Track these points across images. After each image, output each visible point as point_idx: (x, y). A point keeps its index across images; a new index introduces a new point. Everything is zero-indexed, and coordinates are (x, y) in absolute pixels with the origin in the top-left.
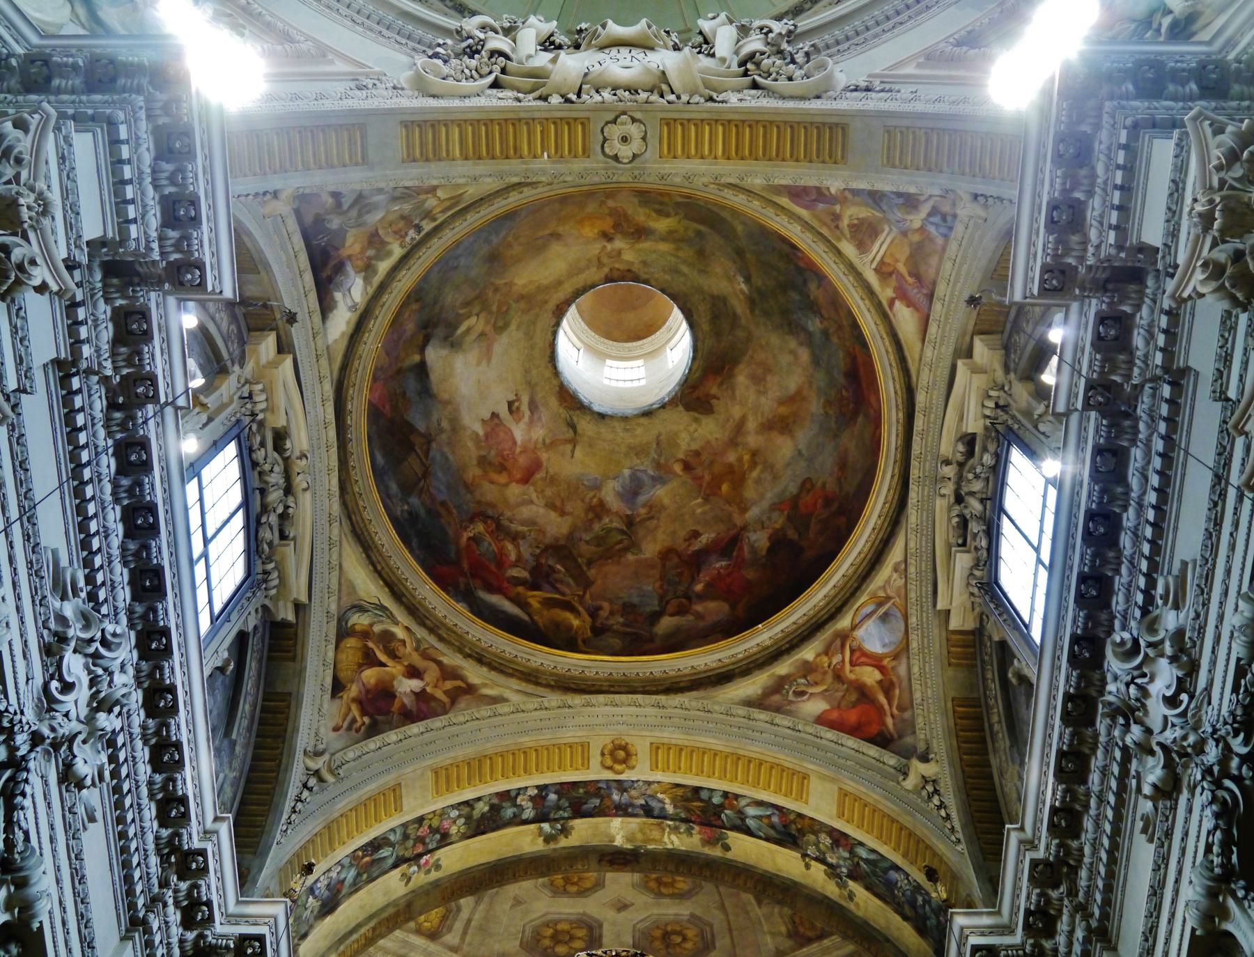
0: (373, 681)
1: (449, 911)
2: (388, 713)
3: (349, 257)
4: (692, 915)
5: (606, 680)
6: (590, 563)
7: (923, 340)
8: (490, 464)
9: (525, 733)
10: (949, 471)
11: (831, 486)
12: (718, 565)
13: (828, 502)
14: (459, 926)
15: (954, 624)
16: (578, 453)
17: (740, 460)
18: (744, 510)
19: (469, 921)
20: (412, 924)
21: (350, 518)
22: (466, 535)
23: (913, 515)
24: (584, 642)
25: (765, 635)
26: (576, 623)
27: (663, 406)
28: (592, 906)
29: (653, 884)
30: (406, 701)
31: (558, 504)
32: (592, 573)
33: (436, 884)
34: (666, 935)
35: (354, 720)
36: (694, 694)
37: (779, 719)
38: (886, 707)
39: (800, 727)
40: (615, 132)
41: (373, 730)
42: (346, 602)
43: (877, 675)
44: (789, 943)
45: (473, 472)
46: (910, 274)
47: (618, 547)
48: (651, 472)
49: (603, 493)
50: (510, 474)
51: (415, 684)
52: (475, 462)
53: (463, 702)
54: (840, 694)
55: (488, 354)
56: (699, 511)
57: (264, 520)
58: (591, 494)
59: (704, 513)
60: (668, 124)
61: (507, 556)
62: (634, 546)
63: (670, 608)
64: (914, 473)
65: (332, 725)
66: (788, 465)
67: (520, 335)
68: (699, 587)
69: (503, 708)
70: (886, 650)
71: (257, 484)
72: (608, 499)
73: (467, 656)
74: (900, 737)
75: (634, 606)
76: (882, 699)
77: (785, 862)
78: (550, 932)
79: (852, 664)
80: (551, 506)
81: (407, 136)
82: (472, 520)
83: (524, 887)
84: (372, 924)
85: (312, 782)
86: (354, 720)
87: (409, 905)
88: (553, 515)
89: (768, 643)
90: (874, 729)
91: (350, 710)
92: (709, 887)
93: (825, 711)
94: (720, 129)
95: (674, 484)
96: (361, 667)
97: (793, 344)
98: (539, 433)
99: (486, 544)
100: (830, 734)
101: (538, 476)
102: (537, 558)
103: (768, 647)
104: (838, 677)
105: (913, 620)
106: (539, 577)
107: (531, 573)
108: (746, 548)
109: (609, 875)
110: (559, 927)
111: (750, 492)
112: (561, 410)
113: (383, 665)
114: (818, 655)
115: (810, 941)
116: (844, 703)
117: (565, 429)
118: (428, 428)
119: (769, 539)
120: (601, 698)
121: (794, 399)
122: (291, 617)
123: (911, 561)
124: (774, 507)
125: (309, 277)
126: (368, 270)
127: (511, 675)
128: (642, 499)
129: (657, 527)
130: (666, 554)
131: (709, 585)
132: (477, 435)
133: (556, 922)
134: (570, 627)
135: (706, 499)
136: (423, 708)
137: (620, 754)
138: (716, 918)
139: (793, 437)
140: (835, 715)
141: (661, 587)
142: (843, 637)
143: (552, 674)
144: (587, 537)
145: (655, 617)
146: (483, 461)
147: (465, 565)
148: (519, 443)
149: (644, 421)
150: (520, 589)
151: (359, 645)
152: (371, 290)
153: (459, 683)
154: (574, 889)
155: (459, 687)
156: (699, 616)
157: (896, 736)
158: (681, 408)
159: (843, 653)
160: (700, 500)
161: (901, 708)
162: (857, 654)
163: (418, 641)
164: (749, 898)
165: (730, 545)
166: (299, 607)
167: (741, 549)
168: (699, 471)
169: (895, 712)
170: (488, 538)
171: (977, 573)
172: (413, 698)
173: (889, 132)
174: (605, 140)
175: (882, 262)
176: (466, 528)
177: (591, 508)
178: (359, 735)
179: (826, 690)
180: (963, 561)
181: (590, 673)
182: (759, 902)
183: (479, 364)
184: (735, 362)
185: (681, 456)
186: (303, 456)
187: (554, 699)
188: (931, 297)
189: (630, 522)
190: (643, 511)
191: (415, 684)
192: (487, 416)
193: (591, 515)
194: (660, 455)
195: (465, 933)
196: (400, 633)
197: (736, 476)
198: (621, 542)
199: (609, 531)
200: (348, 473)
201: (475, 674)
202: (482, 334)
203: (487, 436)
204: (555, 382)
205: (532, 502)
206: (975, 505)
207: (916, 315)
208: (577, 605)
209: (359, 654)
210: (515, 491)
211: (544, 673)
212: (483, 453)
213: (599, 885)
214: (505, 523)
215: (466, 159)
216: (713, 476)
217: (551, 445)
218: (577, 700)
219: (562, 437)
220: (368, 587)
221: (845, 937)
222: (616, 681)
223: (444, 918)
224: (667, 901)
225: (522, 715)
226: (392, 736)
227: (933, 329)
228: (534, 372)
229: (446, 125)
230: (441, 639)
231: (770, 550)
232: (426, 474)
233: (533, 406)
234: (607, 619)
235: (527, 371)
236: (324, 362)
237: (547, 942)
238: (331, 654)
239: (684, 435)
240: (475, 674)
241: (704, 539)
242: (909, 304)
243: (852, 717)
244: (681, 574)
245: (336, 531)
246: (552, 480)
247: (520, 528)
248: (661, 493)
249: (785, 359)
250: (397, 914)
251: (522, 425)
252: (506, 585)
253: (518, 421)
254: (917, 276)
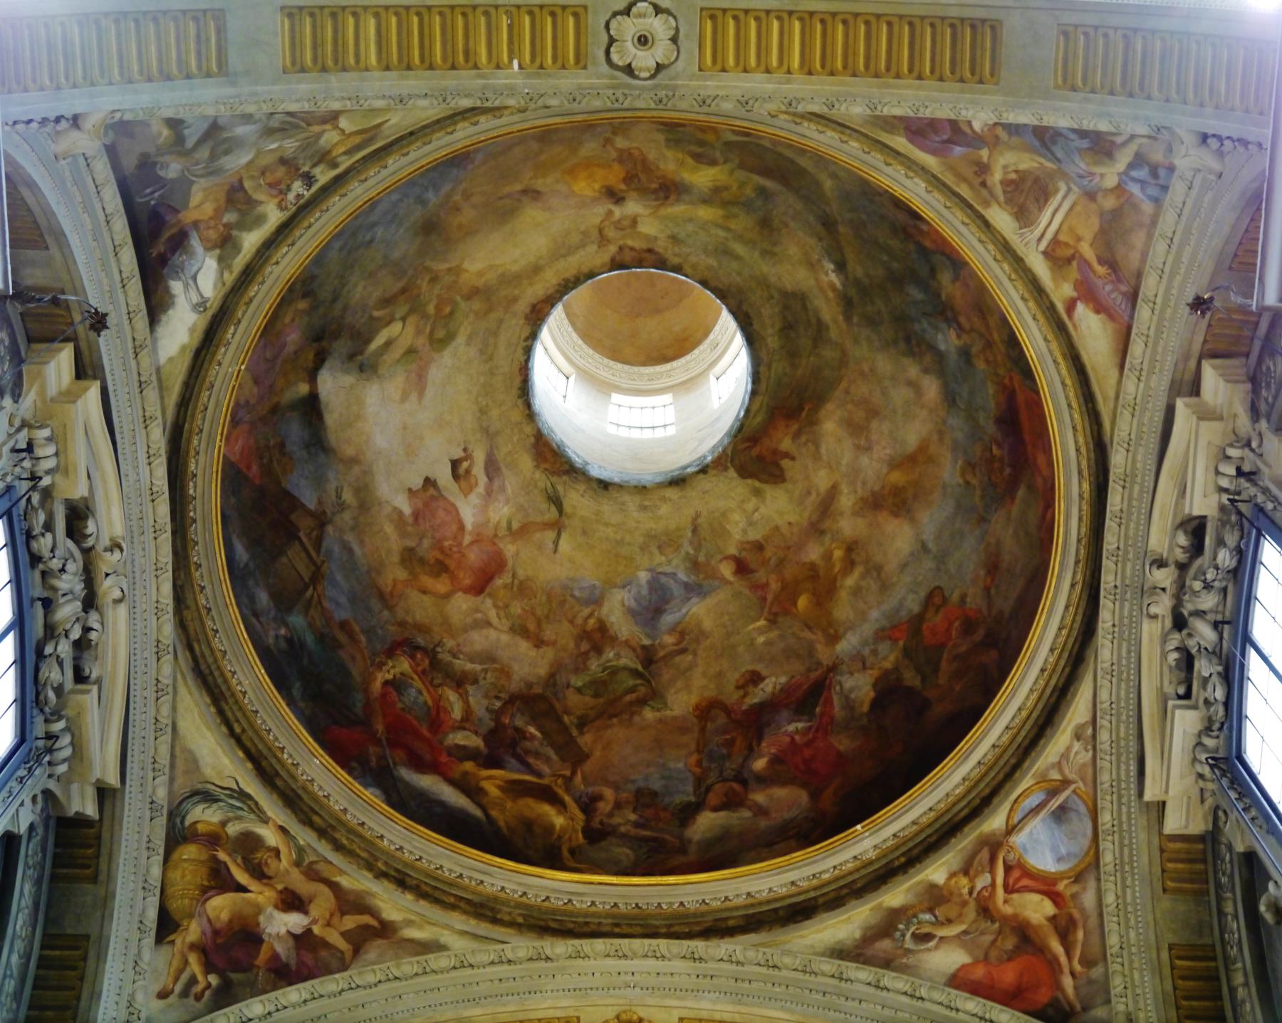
0: (225, 916)
2: (247, 967)
3: (196, 224)
5: (608, 915)
6: (582, 724)
7: (1122, 367)
8: (422, 561)
9: (475, 1001)
10: (1163, 577)
11: (975, 601)
12: (791, 728)
13: (969, 626)
15: (1174, 823)
16: (564, 545)
17: (828, 556)
18: (834, 639)
21: (190, 648)
22: (381, 677)
23: (1105, 649)
24: (572, 852)
25: (866, 842)
26: (559, 821)
27: (704, 470)
30: (280, 948)
31: (532, 627)
32: (585, 740)
35: (193, 981)
36: (752, 938)
37: (888, 978)
38: (1063, 959)
39: (923, 993)
41: (224, 997)
42: (183, 785)
43: (1049, 908)
45: (394, 574)
46: (1101, 261)
47: (628, 698)
48: (682, 576)
49: (605, 610)
50: (453, 578)
51: (295, 921)
52: (396, 558)
53: (374, 950)
54: (988, 938)
55: (419, 382)
56: (761, 639)
57: (49, 649)
58: (587, 611)
59: (769, 643)
60: (713, 17)
61: (448, 712)
62: (654, 696)
63: (713, 799)
64: (1108, 579)
65: (157, 987)
66: (903, 566)
67: (473, 352)
68: (760, 764)
69: (437, 961)
70: (1063, 867)
71: (38, 592)
72: (613, 619)
73: (381, 875)
74: (1085, 1009)
75: (654, 794)
76: (1056, 946)
79: (1008, 889)
80: (520, 630)
81: (292, 30)
82: (390, 652)
86: (193, 981)
88: (524, 646)
89: (872, 855)
90: (1043, 996)
91: (186, 963)
93: (963, 967)
94: (797, 25)
95: (722, 595)
96: (206, 892)
97: (913, 371)
98: (501, 512)
99: (413, 692)
100: (973, 1004)
101: (499, 582)
102: (497, 715)
103: (871, 863)
104: (985, 911)
105: (1105, 818)
106: (500, 746)
107: (486, 739)
108: (835, 698)
111: (842, 609)
112: (538, 475)
113: (243, 889)
114: (952, 875)
116: (994, 954)
117: (544, 506)
118: (320, 503)
119: (875, 685)
120: (600, 944)
121: (913, 460)
122: (91, 810)
123: (1103, 722)
124: (882, 635)
125: (128, 256)
126: (225, 244)
127: (453, 907)
128: (668, 619)
129: (690, 668)
130: (706, 710)
131: (775, 761)
132: (400, 513)
134: (550, 829)
135: (773, 621)
136: (307, 962)
139: (912, 520)
140: (979, 973)
141: (699, 763)
142: (994, 845)
143: (519, 905)
144: (578, 681)
145: (688, 812)
146: (409, 557)
147: (380, 728)
148: (469, 527)
149: (671, 493)
150: (469, 766)
151: (204, 856)
152: (230, 278)
153: (366, 919)
155: (366, 927)
156: (761, 811)
157: (1078, 1007)
158: (732, 473)
159: (992, 872)
160: (762, 623)
161: (1087, 962)
162: (1016, 874)
163: (301, 851)
165: (810, 695)
166: (104, 793)
167: (829, 702)
168: (761, 576)
169: (1078, 968)
170: (418, 683)
171: (1209, 742)
172: (291, 942)
173: (1065, 34)
174: (612, 41)
175: (1055, 241)
176: (380, 666)
177: (584, 635)
178: (200, 1006)
179: (965, 932)
180: (1186, 722)
181: (581, 905)
183: (404, 398)
184: (820, 400)
185: (732, 550)
186: (115, 546)
187: (522, 946)
188: (1133, 297)
189: (649, 657)
190: (669, 640)
191: (295, 921)
192: (417, 483)
193: (585, 646)
194: (698, 548)
196: (270, 837)
197: (821, 584)
198: (632, 690)
199: (614, 672)
200: (188, 574)
201: (393, 904)
202: (411, 351)
203: (416, 515)
204: (528, 430)
205: (489, 624)
206: (1205, 633)
207: (1110, 326)
208: (561, 792)
209: (204, 871)
210: (461, 605)
211: (506, 903)
212: (410, 543)
214: (445, 657)
215: (387, 68)
216: (785, 583)
217: (521, 532)
218: (559, 947)
219: (539, 519)
220: (219, 761)
222: (624, 916)
225: (469, 971)
226: (255, 1007)
227: (1137, 348)
228: (495, 413)
229: (355, 14)
230: (338, 847)
231: (875, 704)
232: (317, 576)
233: (492, 467)
234: (610, 815)
235: (483, 411)
236: (152, 394)
238: (156, 871)
239: (736, 517)
240: (393, 904)
241: (769, 686)
242: (1099, 308)
243: (1008, 975)
244: (730, 743)
245: (167, 669)
246: (523, 589)
247: (469, 666)
248: (701, 611)
249: (900, 395)
251: (474, 498)
252: (444, 759)
253: (466, 493)
254: (1112, 264)
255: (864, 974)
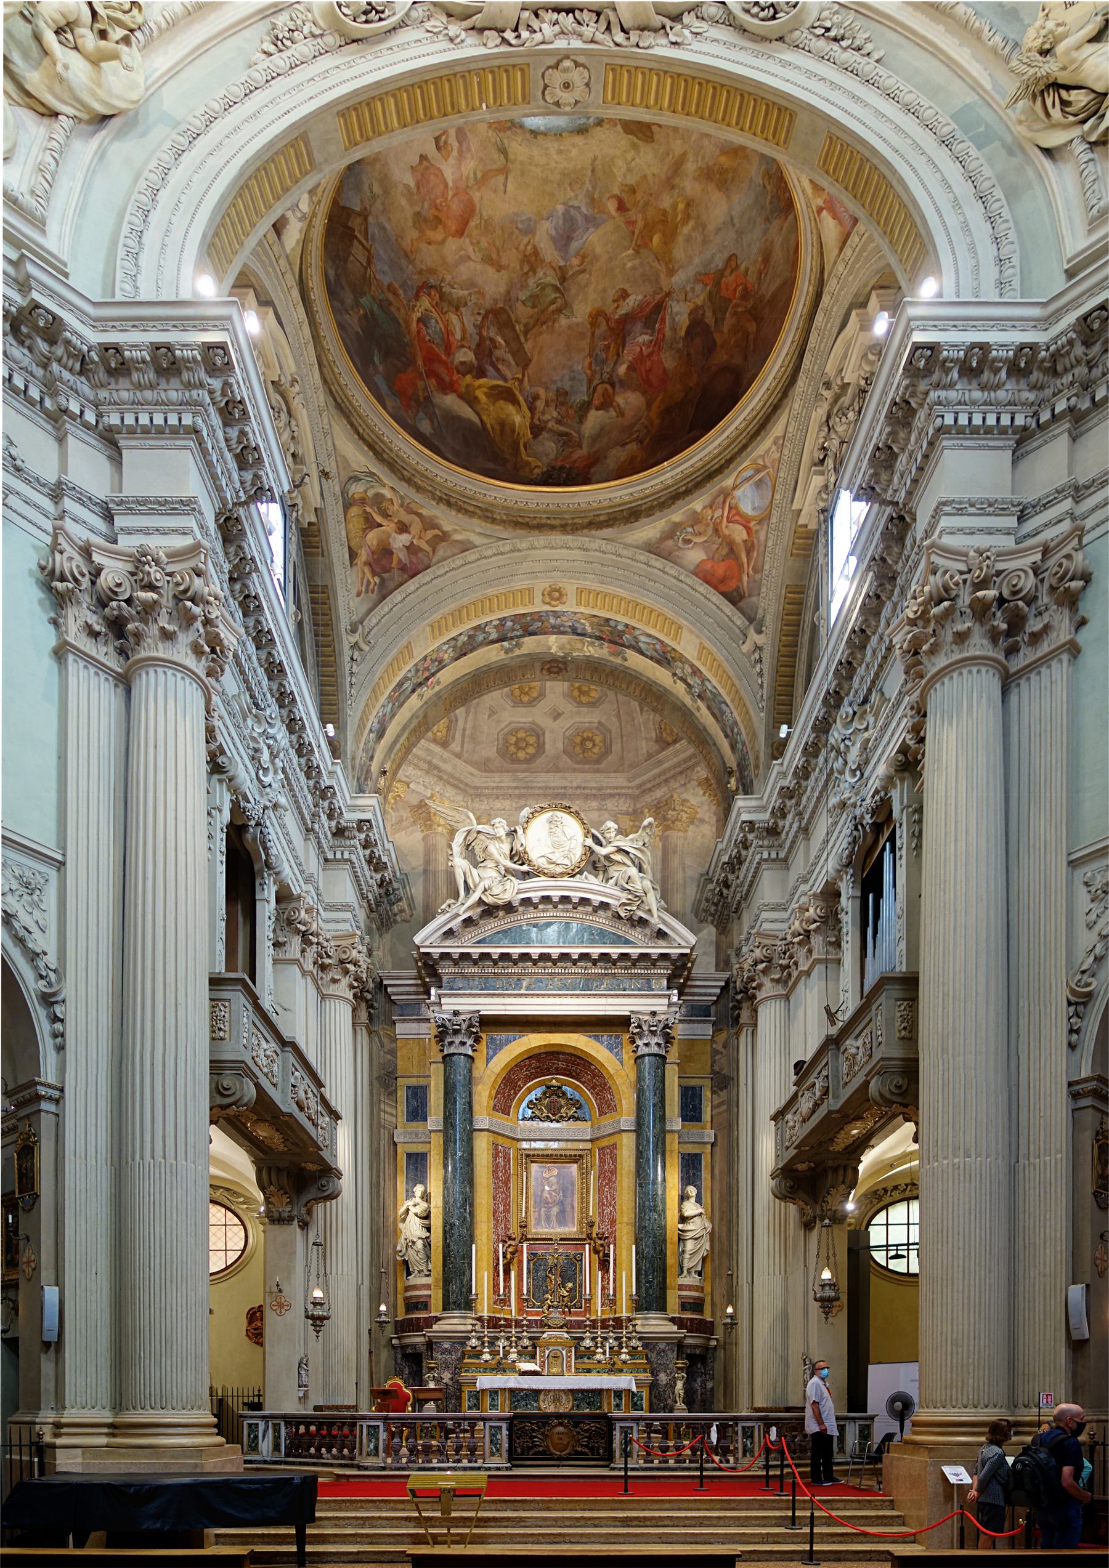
1: (451, 721)
4: (600, 723)
5: (545, 512)
14: (458, 735)
19: (464, 730)
20: (430, 734)
28: (537, 715)
29: (576, 693)
33: (438, 695)
34: (584, 740)
44: (656, 747)
50: (445, 227)
78: (513, 740)
83: (495, 697)
84: (406, 735)
87: (425, 717)
92: (611, 694)
101: (472, 224)
109: (548, 684)
110: (521, 735)
115: (668, 744)
117: (496, 156)
133: (517, 730)
137: (555, 594)
138: (613, 725)
148: (450, 184)
154: (525, 699)
164: (635, 704)
182: (642, 710)
195: (463, 742)
213: (542, 694)
219: (494, 167)
221: (690, 741)
223: (449, 728)
224: (584, 709)
237: (512, 749)
250: (419, 725)
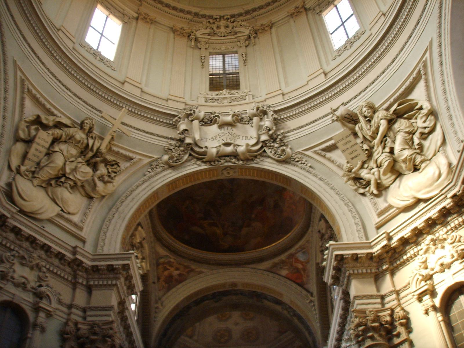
28: (229, 324)
36: (253, 266)
40: (225, 172)
41: (169, 289)
51: (177, 272)
68: (253, 216)
69: (201, 275)
70: (304, 261)
73: (191, 260)
77: (278, 308)
83: (212, 319)
85: (157, 310)
104: (292, 265)
142: (292, 256)
153: (189, 269)
191: (177, 272)
196: (172, 260)
213: (230, 316)
220: (162, 251)
226: (174, 290)
230: (184, 257)
255: (271, 274)
